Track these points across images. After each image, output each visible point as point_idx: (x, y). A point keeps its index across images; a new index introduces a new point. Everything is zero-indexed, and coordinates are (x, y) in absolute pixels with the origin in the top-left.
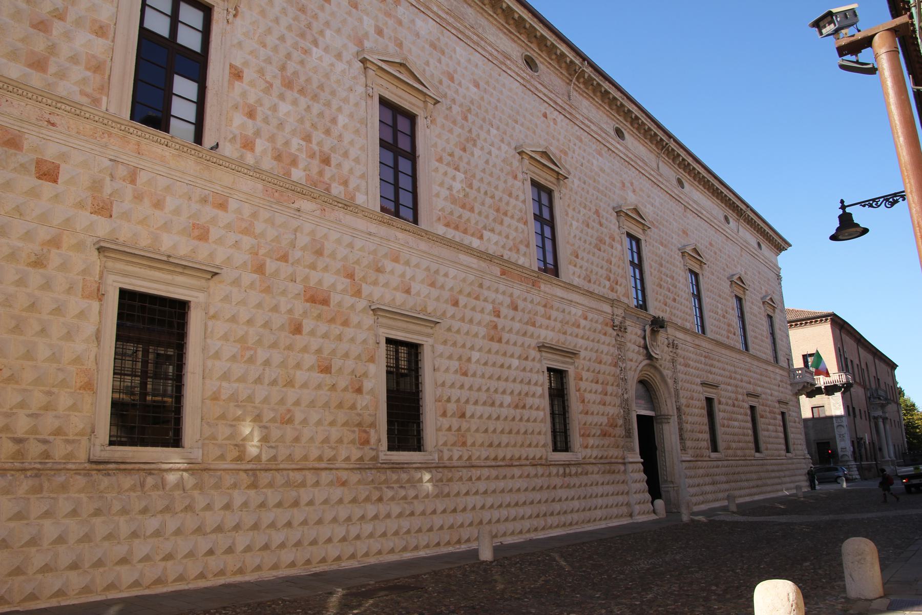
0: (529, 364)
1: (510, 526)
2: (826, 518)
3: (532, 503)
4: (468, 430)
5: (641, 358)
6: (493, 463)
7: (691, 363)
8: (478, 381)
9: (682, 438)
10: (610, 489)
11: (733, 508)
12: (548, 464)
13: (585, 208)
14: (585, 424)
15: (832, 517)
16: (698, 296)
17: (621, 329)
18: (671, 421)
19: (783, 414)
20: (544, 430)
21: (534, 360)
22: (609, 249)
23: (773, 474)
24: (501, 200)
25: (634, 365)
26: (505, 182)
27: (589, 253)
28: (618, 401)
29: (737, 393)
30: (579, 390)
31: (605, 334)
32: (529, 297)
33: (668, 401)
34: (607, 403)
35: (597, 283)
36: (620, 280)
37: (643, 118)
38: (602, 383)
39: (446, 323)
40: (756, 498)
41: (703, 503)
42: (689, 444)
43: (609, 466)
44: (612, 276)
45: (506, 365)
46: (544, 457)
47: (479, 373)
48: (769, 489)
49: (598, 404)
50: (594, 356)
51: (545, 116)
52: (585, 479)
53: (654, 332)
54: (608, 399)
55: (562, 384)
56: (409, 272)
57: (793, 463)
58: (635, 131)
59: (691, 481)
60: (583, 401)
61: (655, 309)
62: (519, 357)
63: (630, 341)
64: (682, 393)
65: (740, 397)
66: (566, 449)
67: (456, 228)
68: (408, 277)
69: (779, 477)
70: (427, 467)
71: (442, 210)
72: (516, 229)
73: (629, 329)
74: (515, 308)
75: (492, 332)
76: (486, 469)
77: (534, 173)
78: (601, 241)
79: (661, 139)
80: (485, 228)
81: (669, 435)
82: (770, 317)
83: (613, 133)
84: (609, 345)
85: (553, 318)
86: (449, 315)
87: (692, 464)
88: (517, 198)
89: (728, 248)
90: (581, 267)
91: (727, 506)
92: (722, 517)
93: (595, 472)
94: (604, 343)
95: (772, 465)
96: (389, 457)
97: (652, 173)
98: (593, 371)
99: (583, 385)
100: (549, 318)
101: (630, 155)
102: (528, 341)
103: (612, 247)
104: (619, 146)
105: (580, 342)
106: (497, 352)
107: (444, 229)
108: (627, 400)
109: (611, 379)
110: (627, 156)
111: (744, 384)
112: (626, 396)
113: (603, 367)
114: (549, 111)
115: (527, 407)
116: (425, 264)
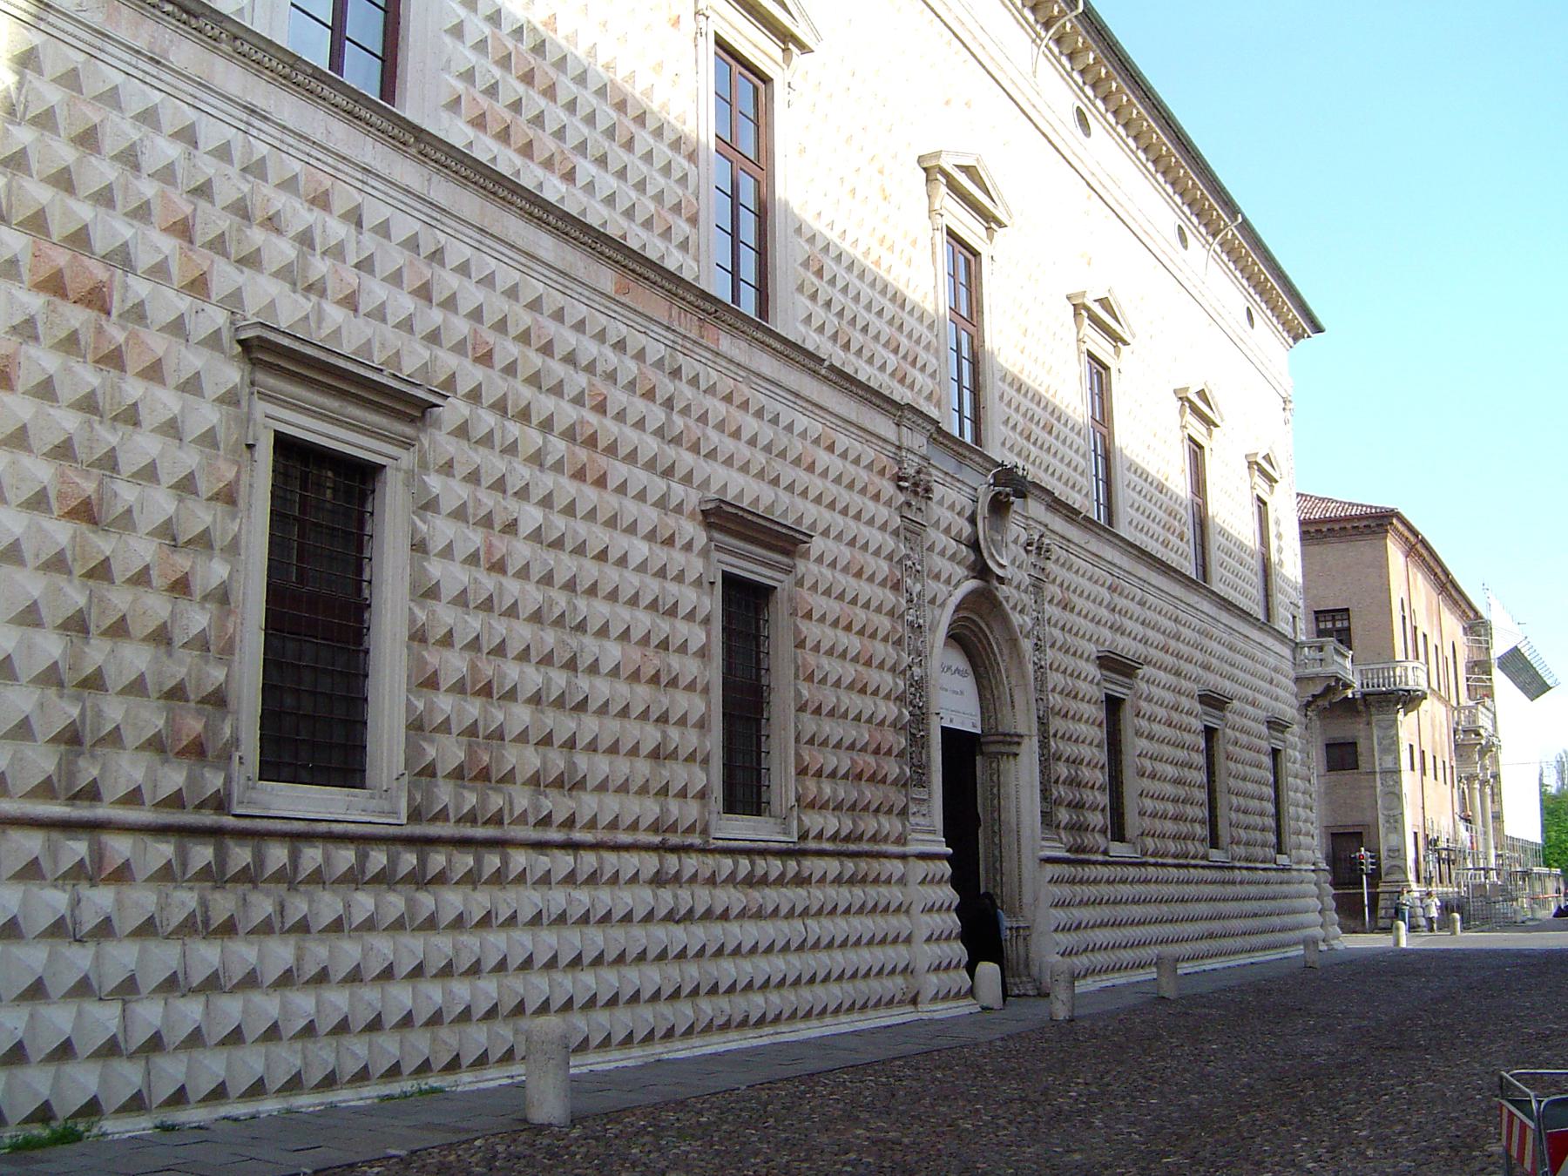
0: (678, 558)
3: (662, 956)
21: (688, 547)
39: (454, 411)
45: (614, 554)
63: (937, 524)
73: (938, 491)
90: (828, 304)
94: (871, 522)
106: (591, 515)
107: (471, 133)
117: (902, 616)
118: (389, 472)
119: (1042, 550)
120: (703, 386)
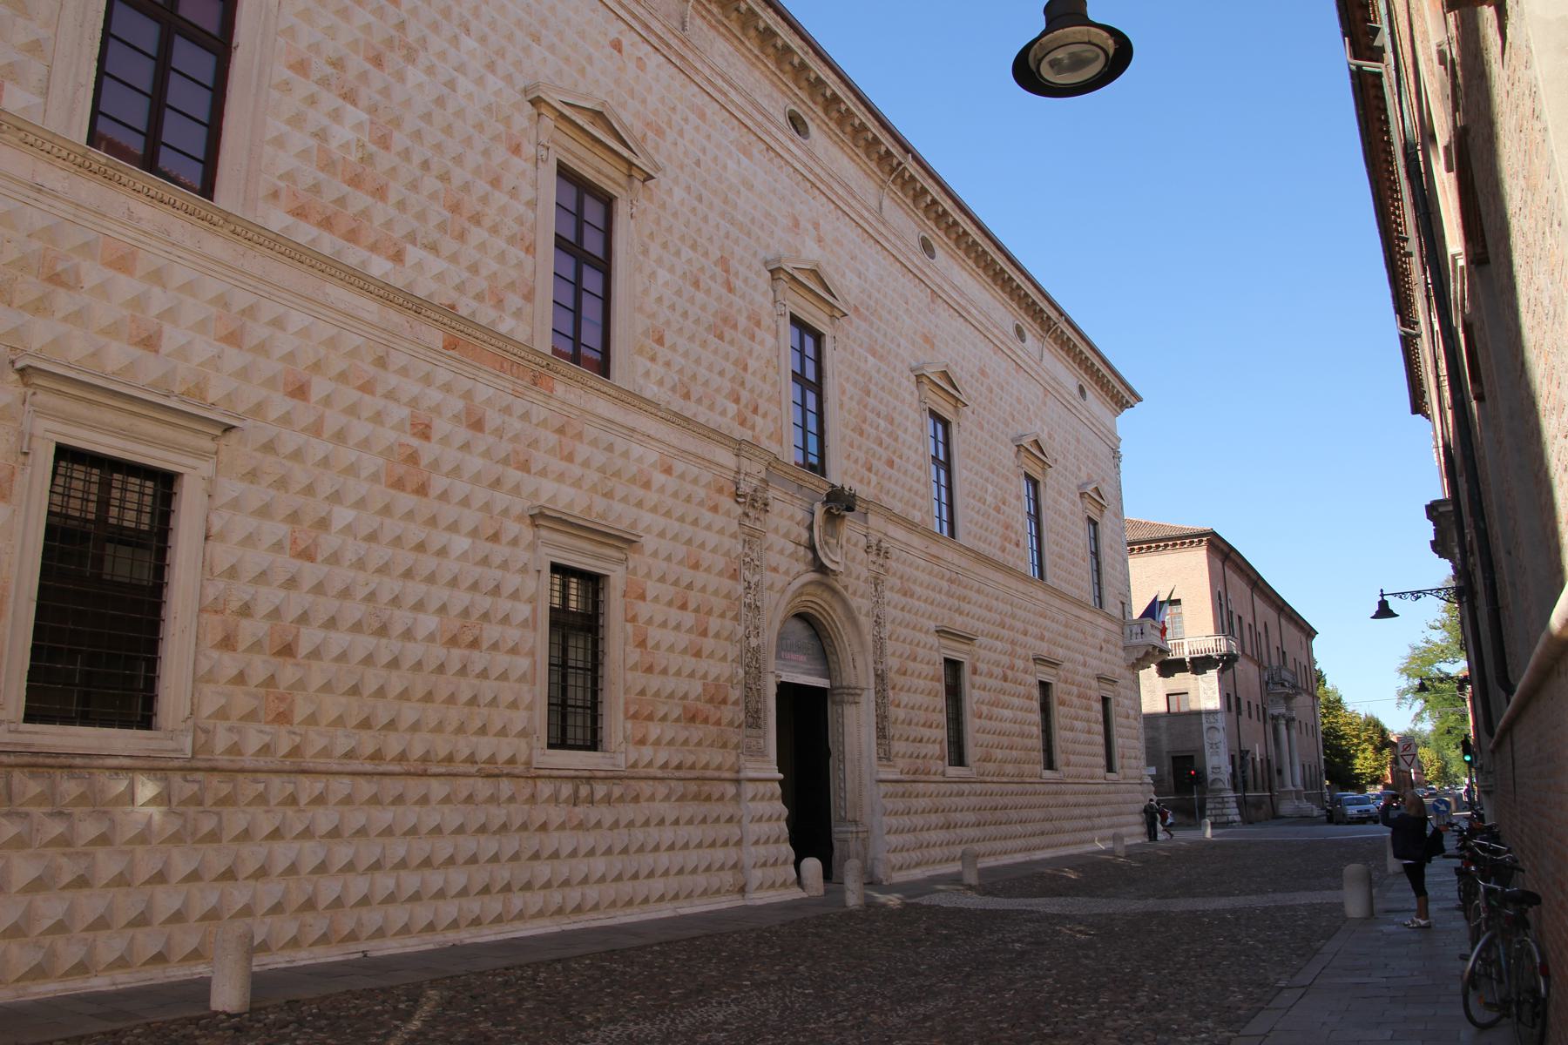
1: (399, 915)
2: (1137, 906)
4: (300, 685)
5: (801, 567)
6: (369, 767)
7: (918, 590)
8: (342, 576)
9: (882, 733)
10: (695, 833)
11: (971, 878)
13: (694, 247)
14: (642, 692)
15: (1151, 904)
16: (946, 465)
17: (754, 503)
18: (863, 699)
19: (1105, 700)
20: (527, 698)
21: (515, 542)
22: (746, 341)
23: (1077, 812)
24: (466, 187)
25: (779, 580)
26: (486, 153)
27: (692, 338)
28: (733, 651)
29: (1012, 654)
30: (634, 619)
31: (715, 509)
32: (519, 406)
34: (705, 653)
35: (706, 402)
36: (763, 406)
37: (850, 101)
38: (697, 610)
40: (1038, 855)
41: (918, 865)
42: (899, 747)
43: (697, 784)
44: (745, 395)
46: (522, 758)
47: (350, 556)
48: (1066, 838)
49: (681, 651)
51: (617, 46)
52: (627, 812)
53: (832, 518)
54: (708, 644)
56: (159, 300)
57: (1117, 792)
58: (832, 125)
59: (893, 821)
60: (642, 644)
61: (838, 473)
62: (474, 533)
63: (776, 530)
64: (890, 646)
65: (1020, 664)
66: (593, 744)
67: (327, 223)
68: (154, 310)
69: (1089, 817)
70: (154, 767)
71: (289, 176)
72: (502, 257)
73: (775, 507)
74: (477, 425)
75: (401, 470)
76: (347, 780)
77: (567, 150)
78: (725, 320)
79: (888, 152)
81: (854, 730)
82: (1093, 523)
83: (782, 120)
84: (721, 532)
85: (579, 459)
86: (273, 414)
87: (900, 788)
88: (514, 192)
89: (1015, 389)
91: (960, 873)
92: (944, 899)
93: (659, 796)
95: (1075, 793)
96: (25, 739)
97: (866, 214)
98: (676, 583)
99: (644, 610)
100: (570, 458)
101: (818, 170)
102: (501, 499)
103: (753, 338)
104: (792, 147)
108: (757, 650)
109: (719, 604)
110: (811, 171)
111: (1030, 640)
112: (754, 642)
113: (700, 578)
114: (628, 39)
115: (657, 669)
119: (881, 551)
120: (534, 421)
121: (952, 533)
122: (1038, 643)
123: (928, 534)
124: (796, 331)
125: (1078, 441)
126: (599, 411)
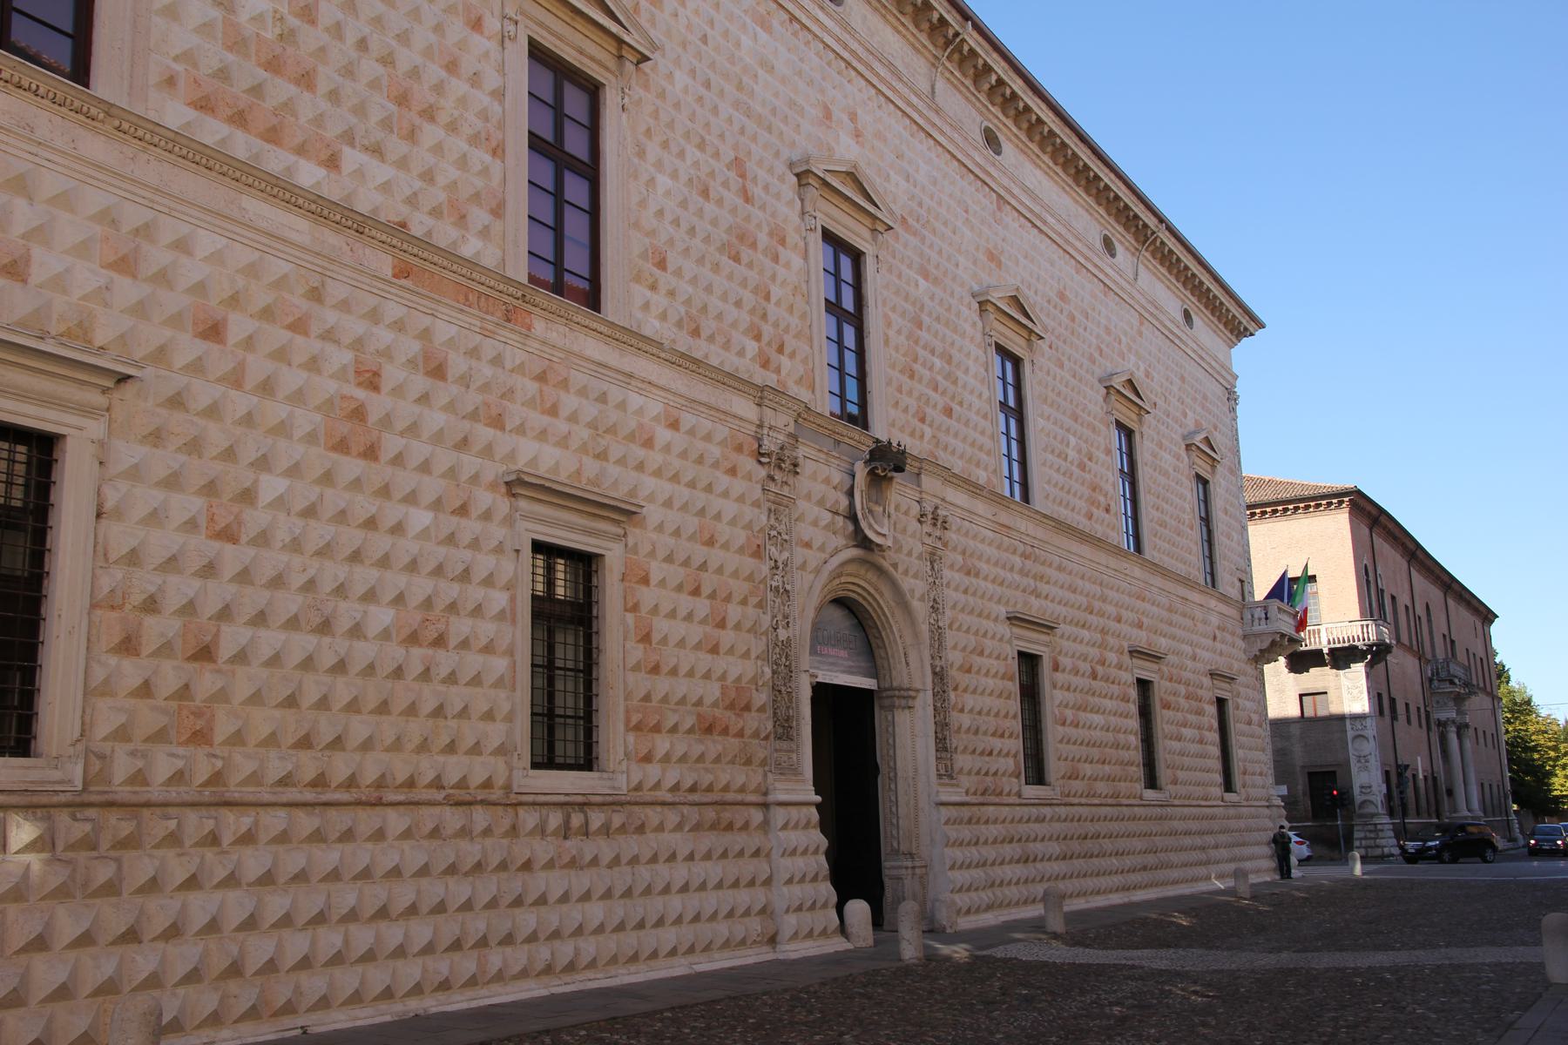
2: (1269, 961)
4: (222, 696)
5: (840, 541)
6: (309, 796)
7: (983, 566)
8: (272, 561)
9: (942, 745)
10: (713, 871)
11: (1056, 924)
12: (514, 802)
13: (701, 146)
14: (647, 698)
15: (1286, 958)
16: (1017, 412)
17: (781, 464)
18: (918, 703)
19: (1221, 703)
20: (506, 707)
21: (487, 516)
22: (768, 262)
24: (415, 73)
25: (813, 557)
26: (438, 29)
27: (701, 261)
28: (758, 646)
29: (1103, 646)
30: (635, 608)
31: (732, 471)
32: (490, 348)
33: (913, 658)
34: (724, 648)
35: (720, 339)
38: (712, 596)
40: (1139, 896)
41: (989, 908)
42: (962, 761)
43: (715, 810)
44: (767, 330)
46: (500, 781)
47: (282, 535)
48: (1175, 874)
49: (697, 644)
50: (692, 523)
52: (631, 845)
53: (877, 481)
54: (727, 637)
55: (588, 591)
57: (1239, 817)
59: (958, 854)
60: (646, 638)
61: (882, 428)
62: (437, 505)
63: (808, 497)
64: (950, 638)
65: (1112, 657)
66: (587, 762)
67: (239, 119)
69: (1203, 849)
70: (32, 804)
71: (187, 57)
72: (463, 162)
73: (807, 468)
75: (344, 428)
76: (282, 813)
77: (541, 24)
78: (742, 238)
79: (942, 20)
80: (349, 137)
81: (908, 740)
82: (1203, 482)
84: (741, 499)
85: (565, 411)
86: (180, 360)
87: (966, 812)
88: (475, 80)
89: (1104, 315)
91: (1042, 919)
93: (669, 825)
95: (1184, 818)
97: (915, 100)
98: (686, 563)
99: (647, 596)
100: (553, 411)
101: (854, 46)
102: (470, 463)
105: (649, 483)
108: (787, 643)
110: (846, 46)
111: (1125, 628)
112: (783, 634)
113: (716, 556)
115: (665, 669)
116: (95, 199)
117: (763, 581)
118: (69, 441)
120: (508, 365)
121: (1026, 497)
122: (1135, 631)
123: (995, 498)
124: (830, 250)
125: (1183, 379)
126: (588, 352)
